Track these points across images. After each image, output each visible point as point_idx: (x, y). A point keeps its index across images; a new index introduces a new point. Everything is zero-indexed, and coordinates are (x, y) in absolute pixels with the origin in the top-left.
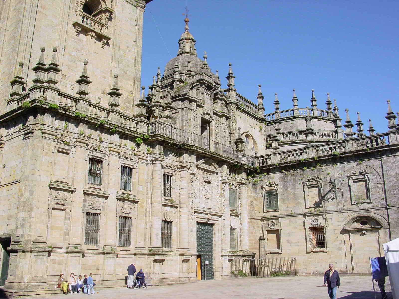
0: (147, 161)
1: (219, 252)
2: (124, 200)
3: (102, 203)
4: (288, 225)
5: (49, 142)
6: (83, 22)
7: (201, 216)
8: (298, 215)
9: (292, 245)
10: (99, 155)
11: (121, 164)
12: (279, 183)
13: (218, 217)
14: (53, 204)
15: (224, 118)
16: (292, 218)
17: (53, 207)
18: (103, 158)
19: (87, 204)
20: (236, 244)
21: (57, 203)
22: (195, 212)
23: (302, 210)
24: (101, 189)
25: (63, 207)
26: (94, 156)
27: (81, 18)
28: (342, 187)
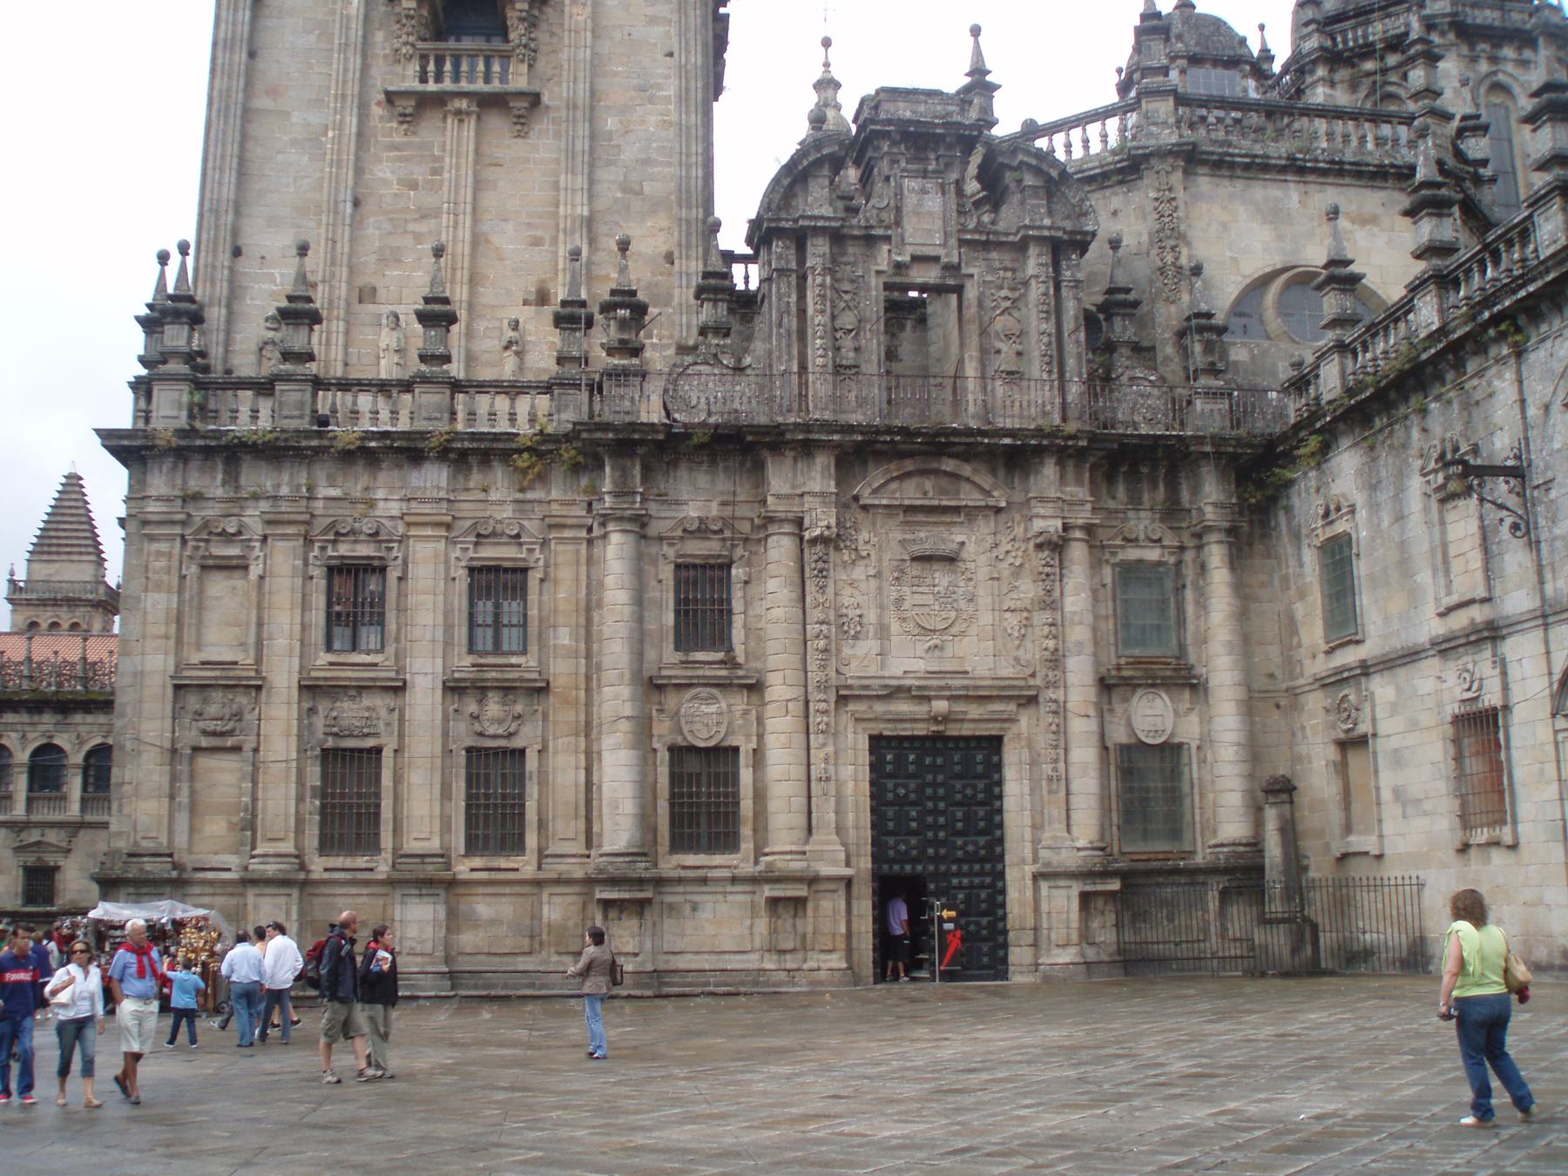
0: (590, 530)
1: (1023, 861)
2: (481, 690)
3: (383, 713)
4: (1394, 709)
5: (163, 546)
6: (423, 80)
7: (886, 712)
8: (1411, 656)
9: (1409, 811)
10: (365, 550)
11: (463, 564)
12: (1359, 498)
13: (1012, 707)
14: (190, 735)
15: (1033, 251)
16: (1401, 673)
17: (196, 744)
18: (381, 558)
19: (319, 722)
20: (1187, 817)
21: (205, 733)
22: (842, 700)
23: (1430, 627)
24: (376, 665)
25: (230, 742)
26: (343, 557)
27: (414, 67)
28: (1550, 475)
